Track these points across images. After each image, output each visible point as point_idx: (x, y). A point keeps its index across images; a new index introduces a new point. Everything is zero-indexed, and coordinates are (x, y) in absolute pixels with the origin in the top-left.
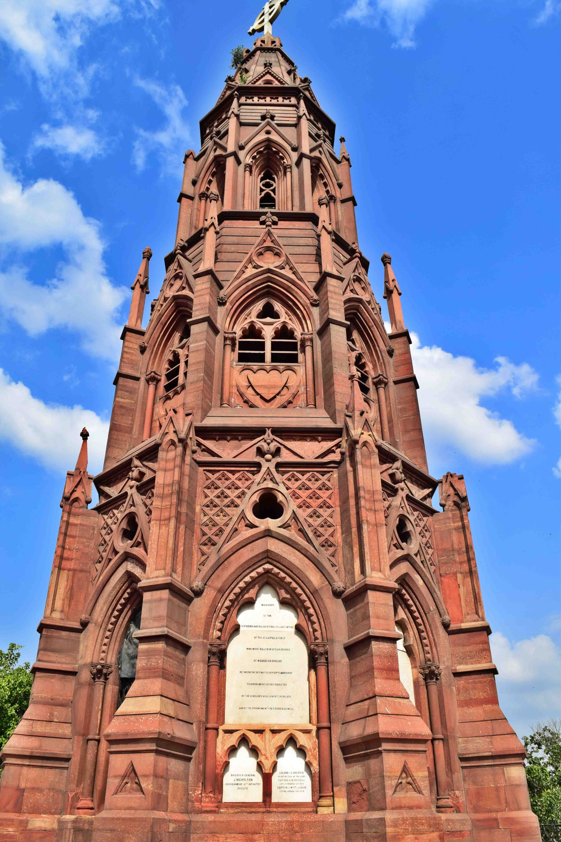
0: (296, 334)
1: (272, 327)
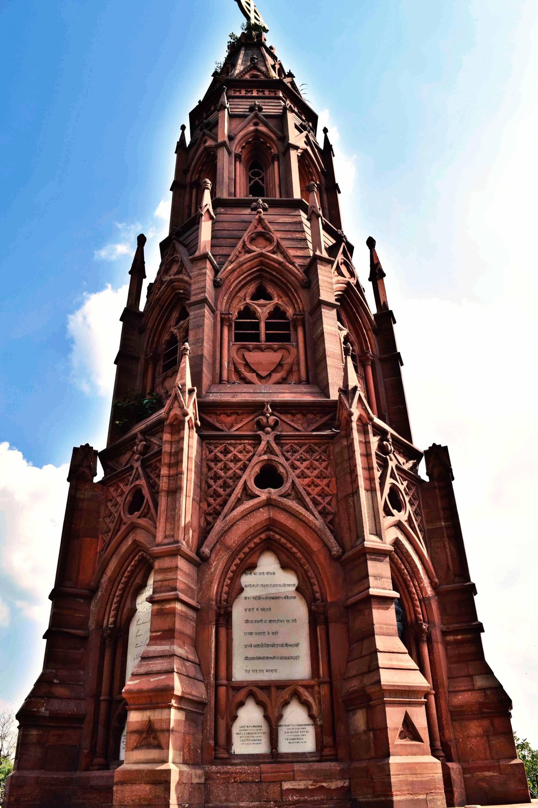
0: (288, 314)
1: (265, 309)
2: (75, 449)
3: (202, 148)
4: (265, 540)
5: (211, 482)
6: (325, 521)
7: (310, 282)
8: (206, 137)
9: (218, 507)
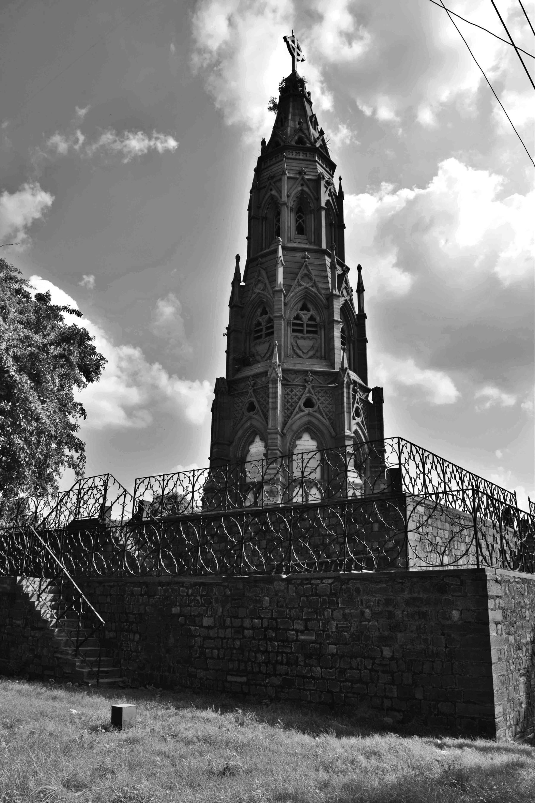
2: (217, 379)
3: (269, 194)
5: (286, 404)
7: (330, 307)
8: (271, 186)
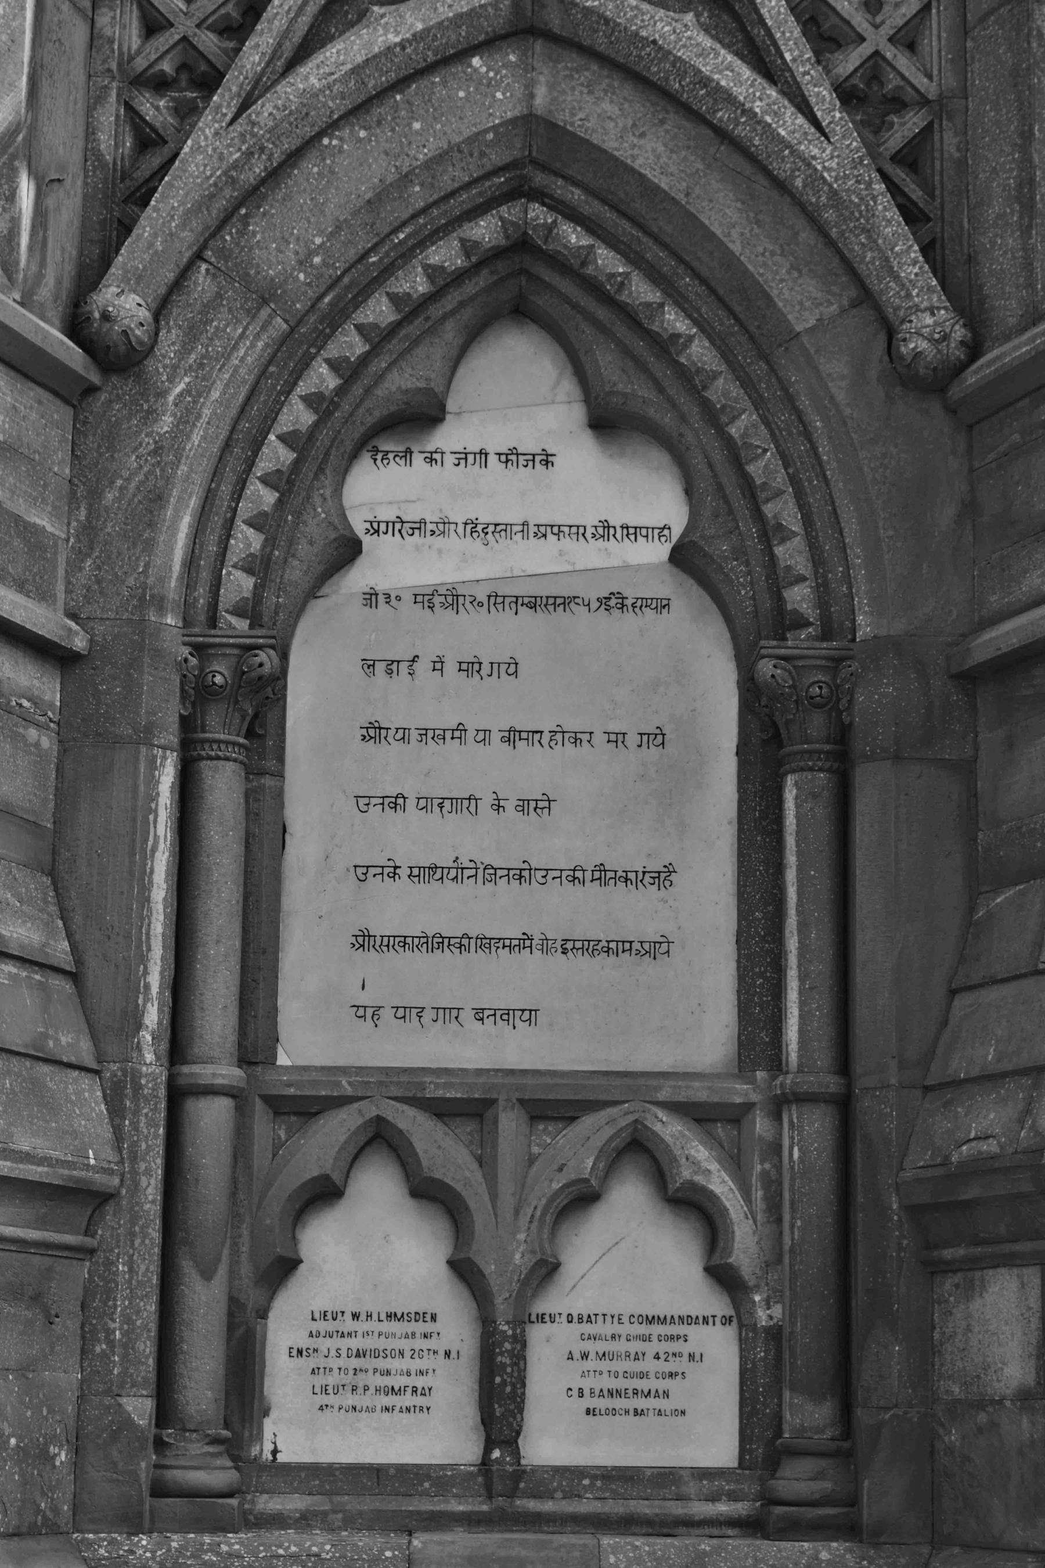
4: (497, 254)
6: (873, 152)
9: (208, 42)
